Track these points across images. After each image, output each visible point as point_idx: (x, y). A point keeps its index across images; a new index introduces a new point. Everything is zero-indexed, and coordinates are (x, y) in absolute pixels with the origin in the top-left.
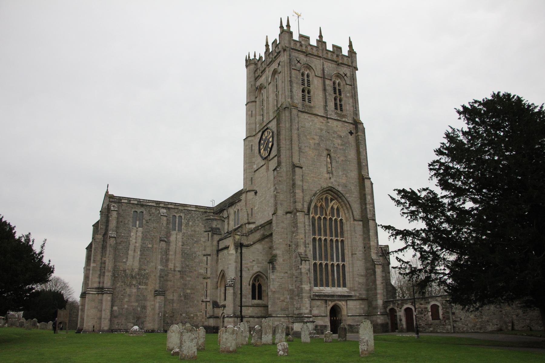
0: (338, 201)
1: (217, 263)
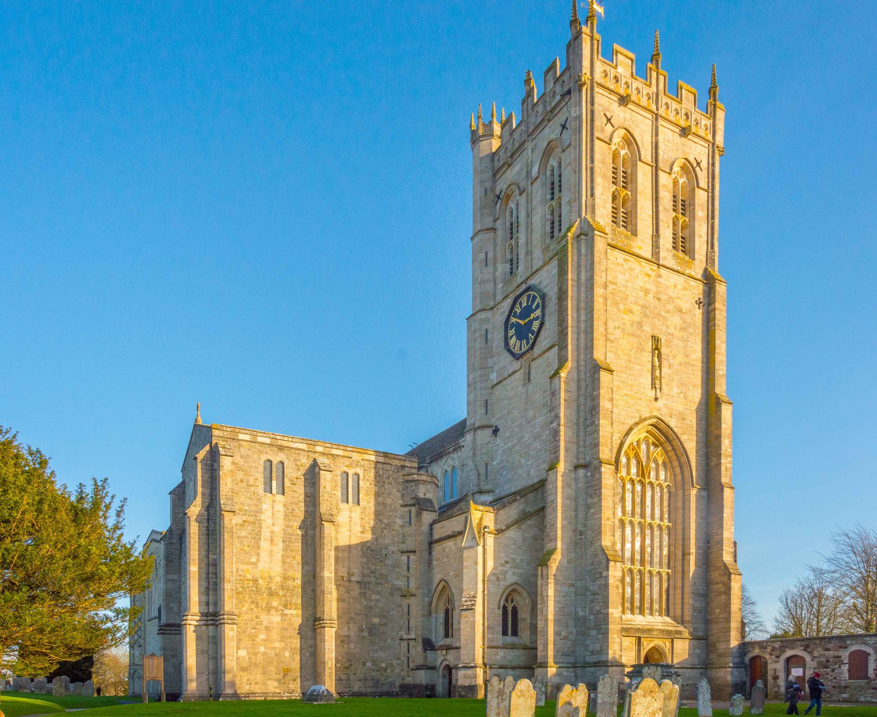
1: (429, 567)
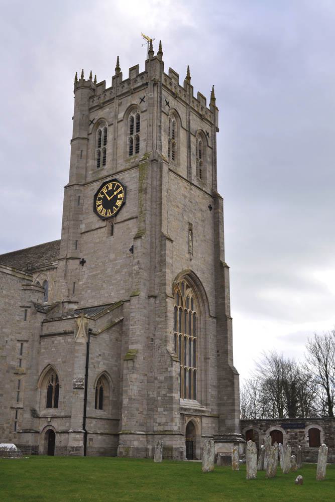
0: (193, 289)
